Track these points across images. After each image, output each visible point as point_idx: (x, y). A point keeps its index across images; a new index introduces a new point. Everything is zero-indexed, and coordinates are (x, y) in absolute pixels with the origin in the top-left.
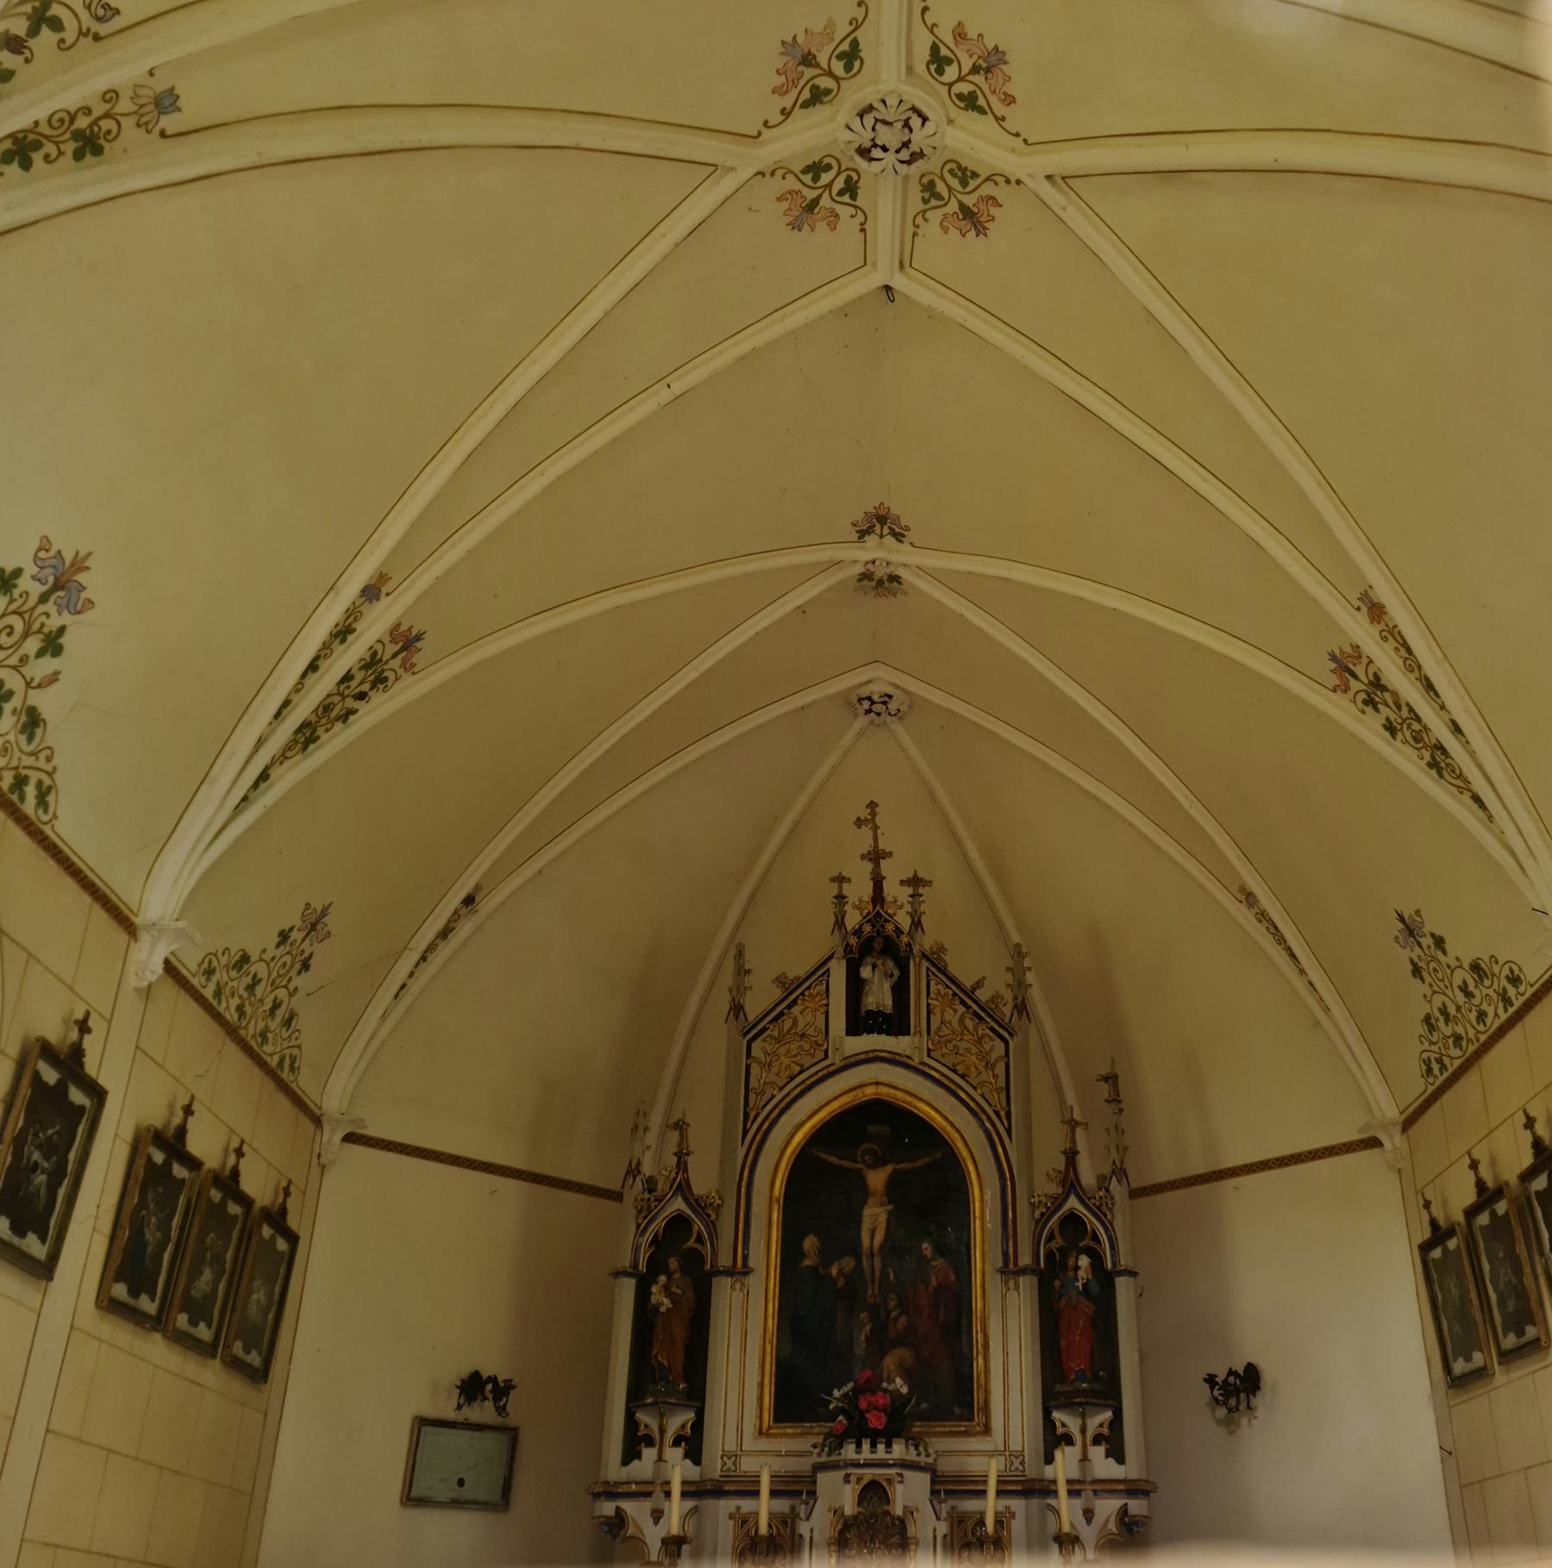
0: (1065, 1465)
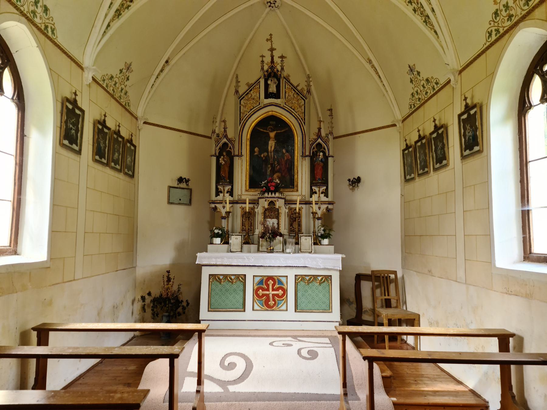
0: (315, 198)
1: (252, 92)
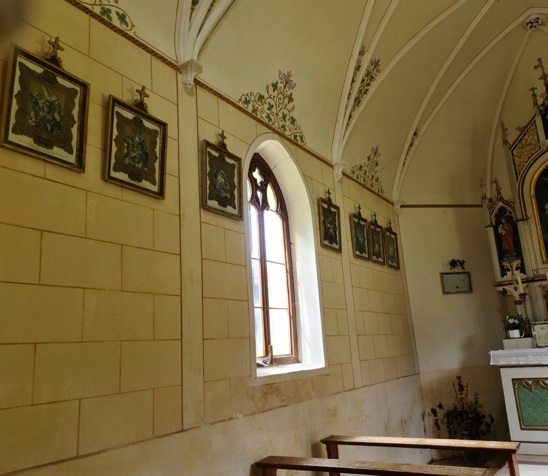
1: (526, 137)
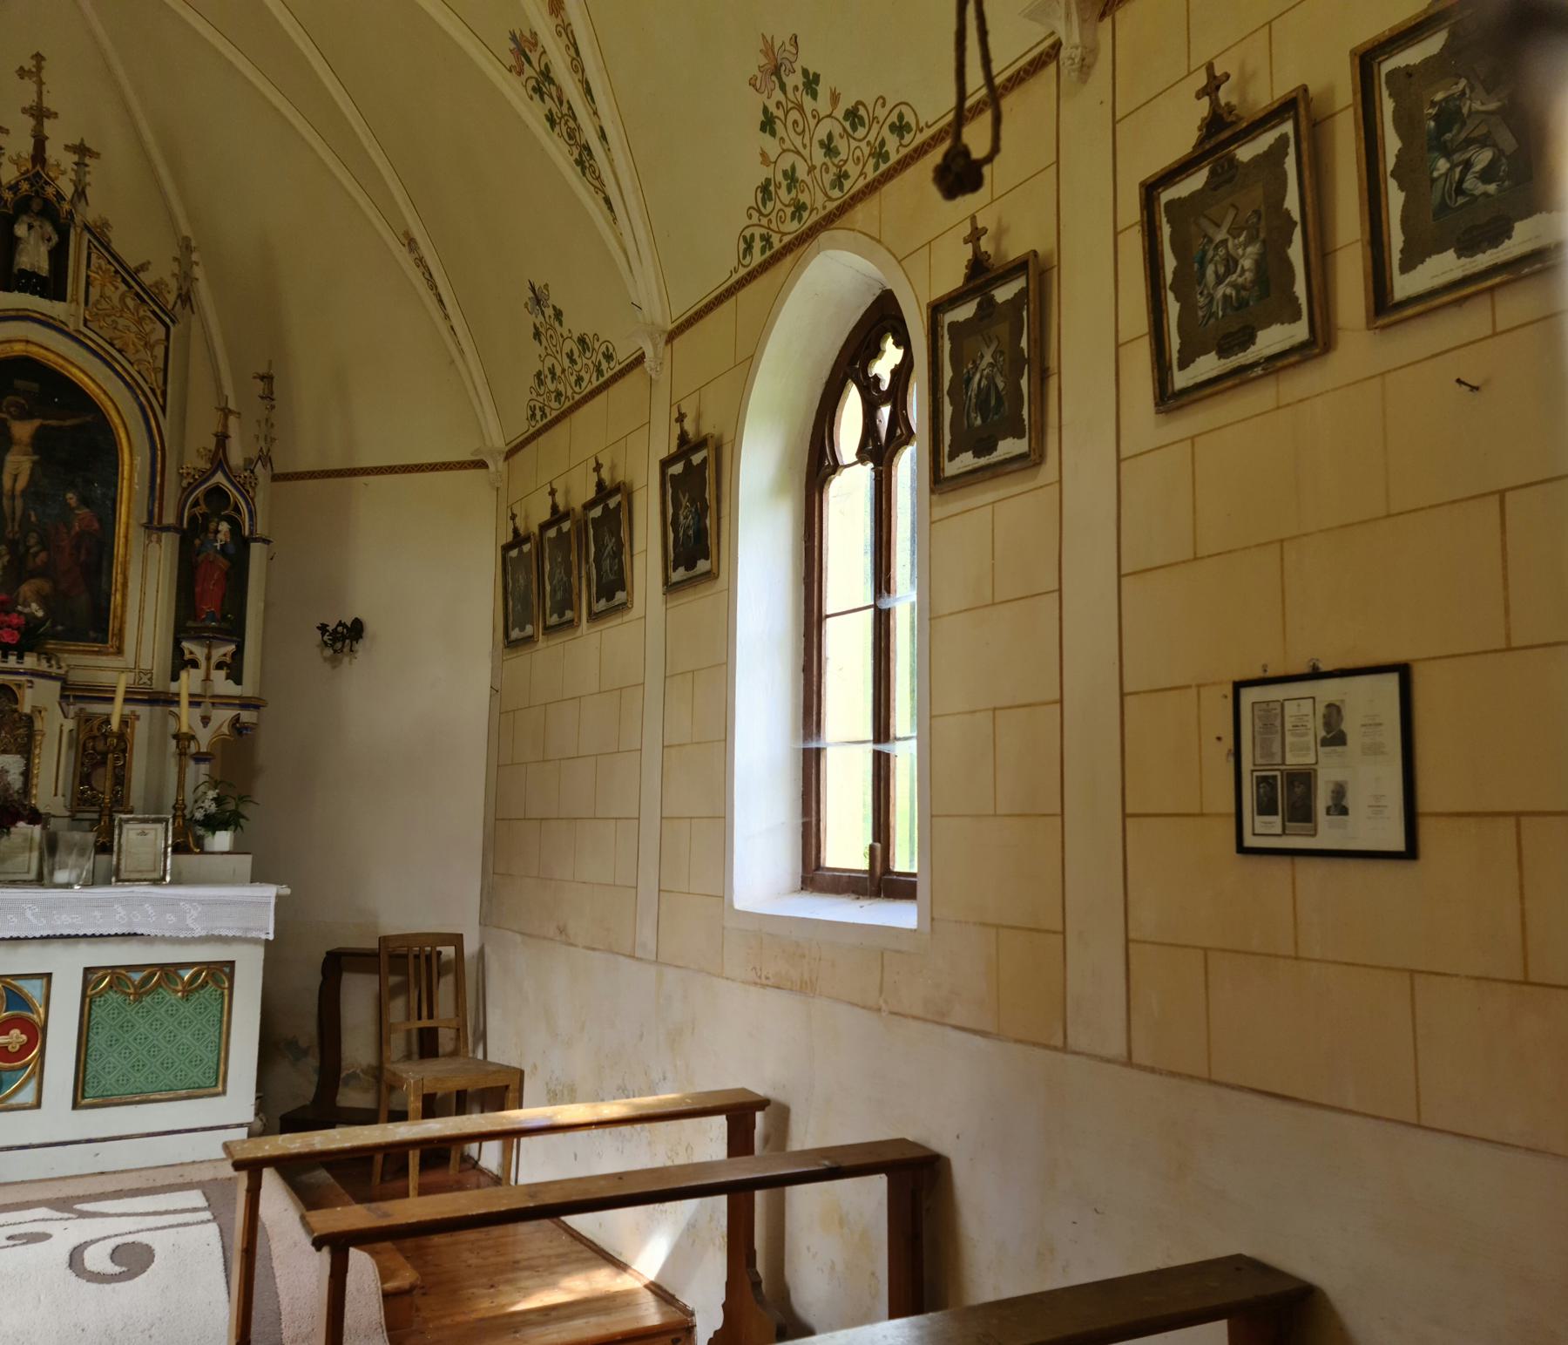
0: (189, 682)
